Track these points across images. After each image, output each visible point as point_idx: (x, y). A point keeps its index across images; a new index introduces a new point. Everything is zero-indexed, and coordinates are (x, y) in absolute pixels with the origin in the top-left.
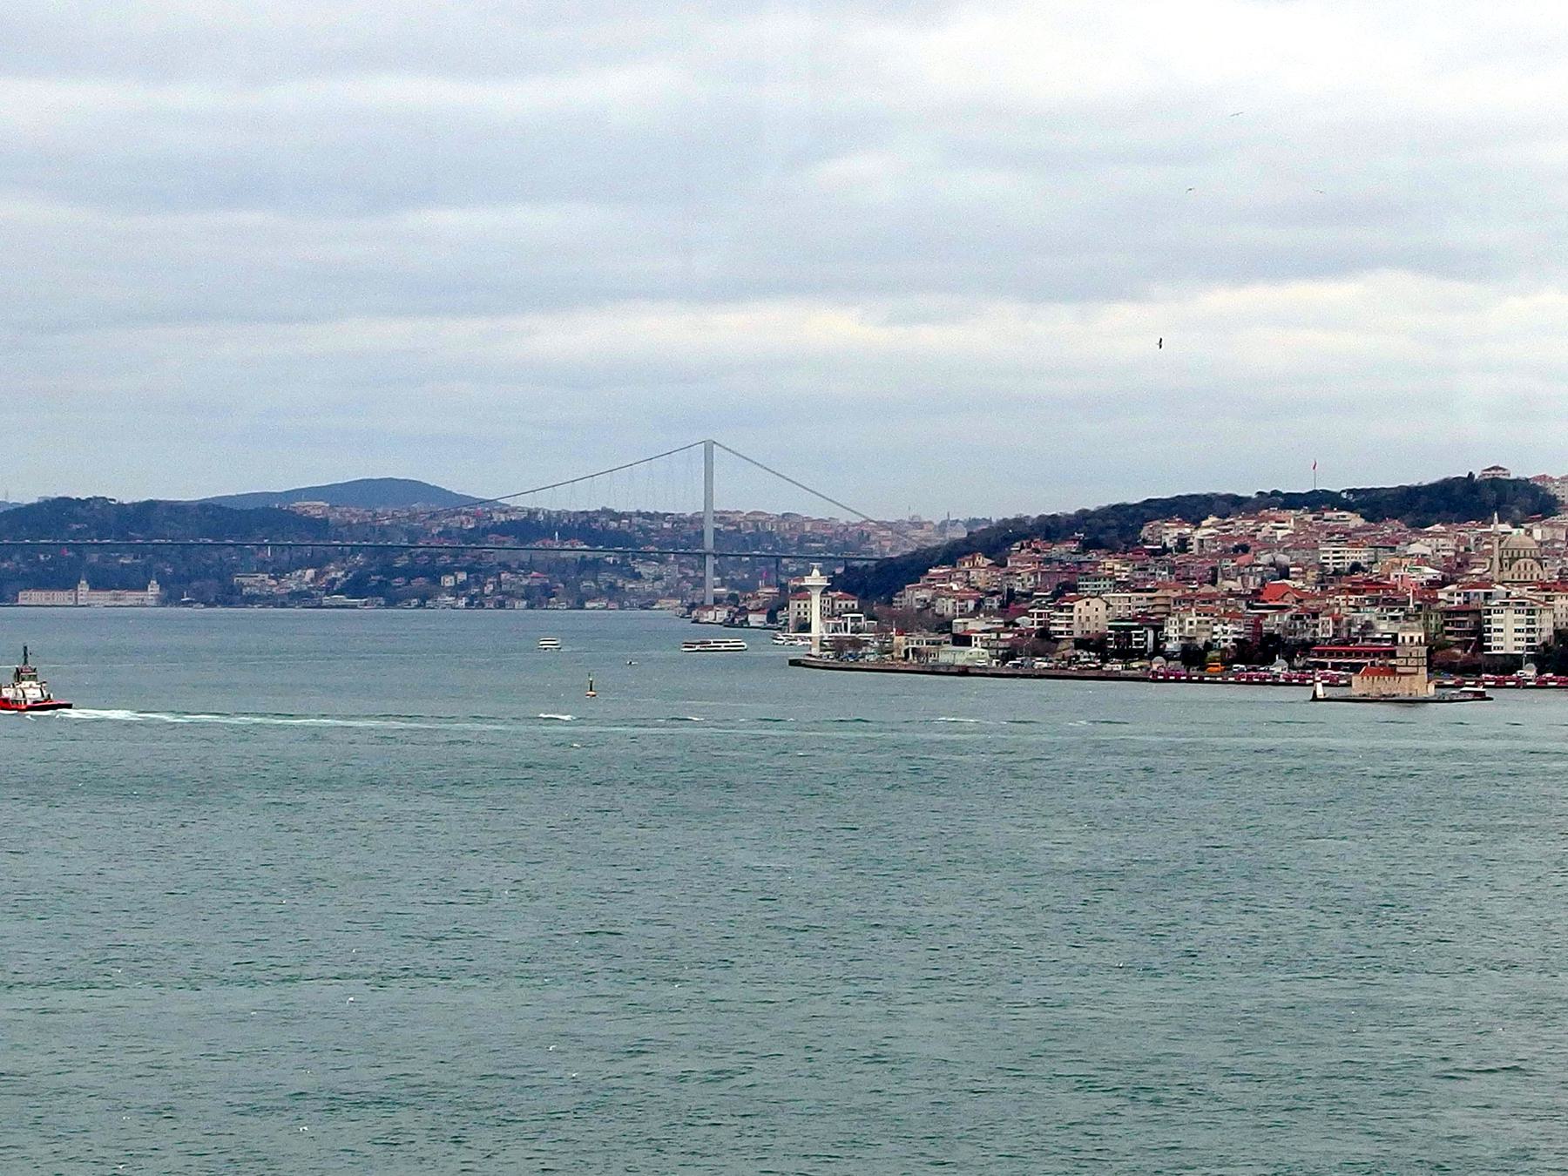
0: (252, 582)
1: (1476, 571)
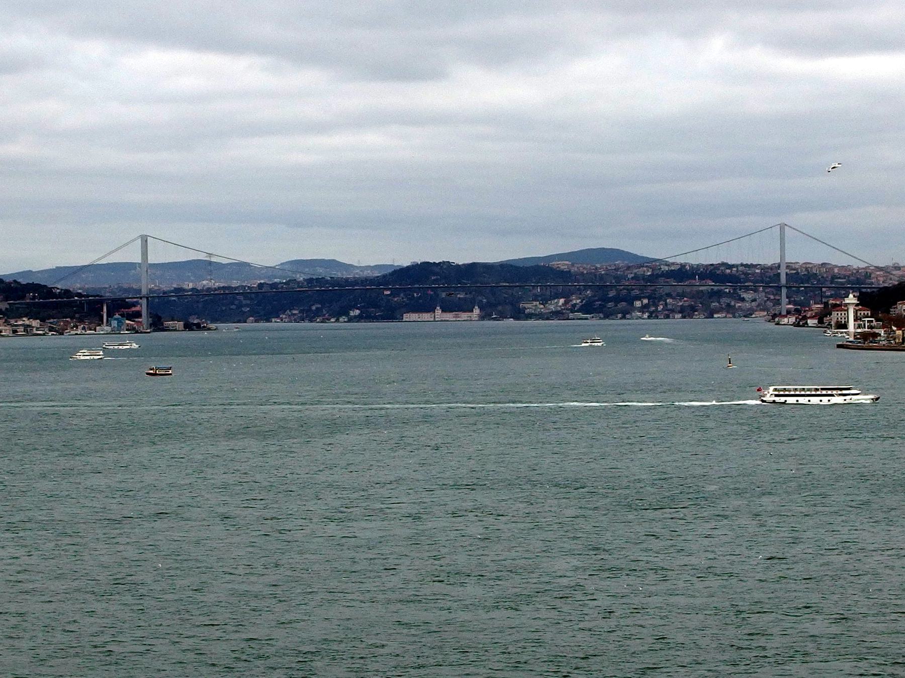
0: (530, 306)
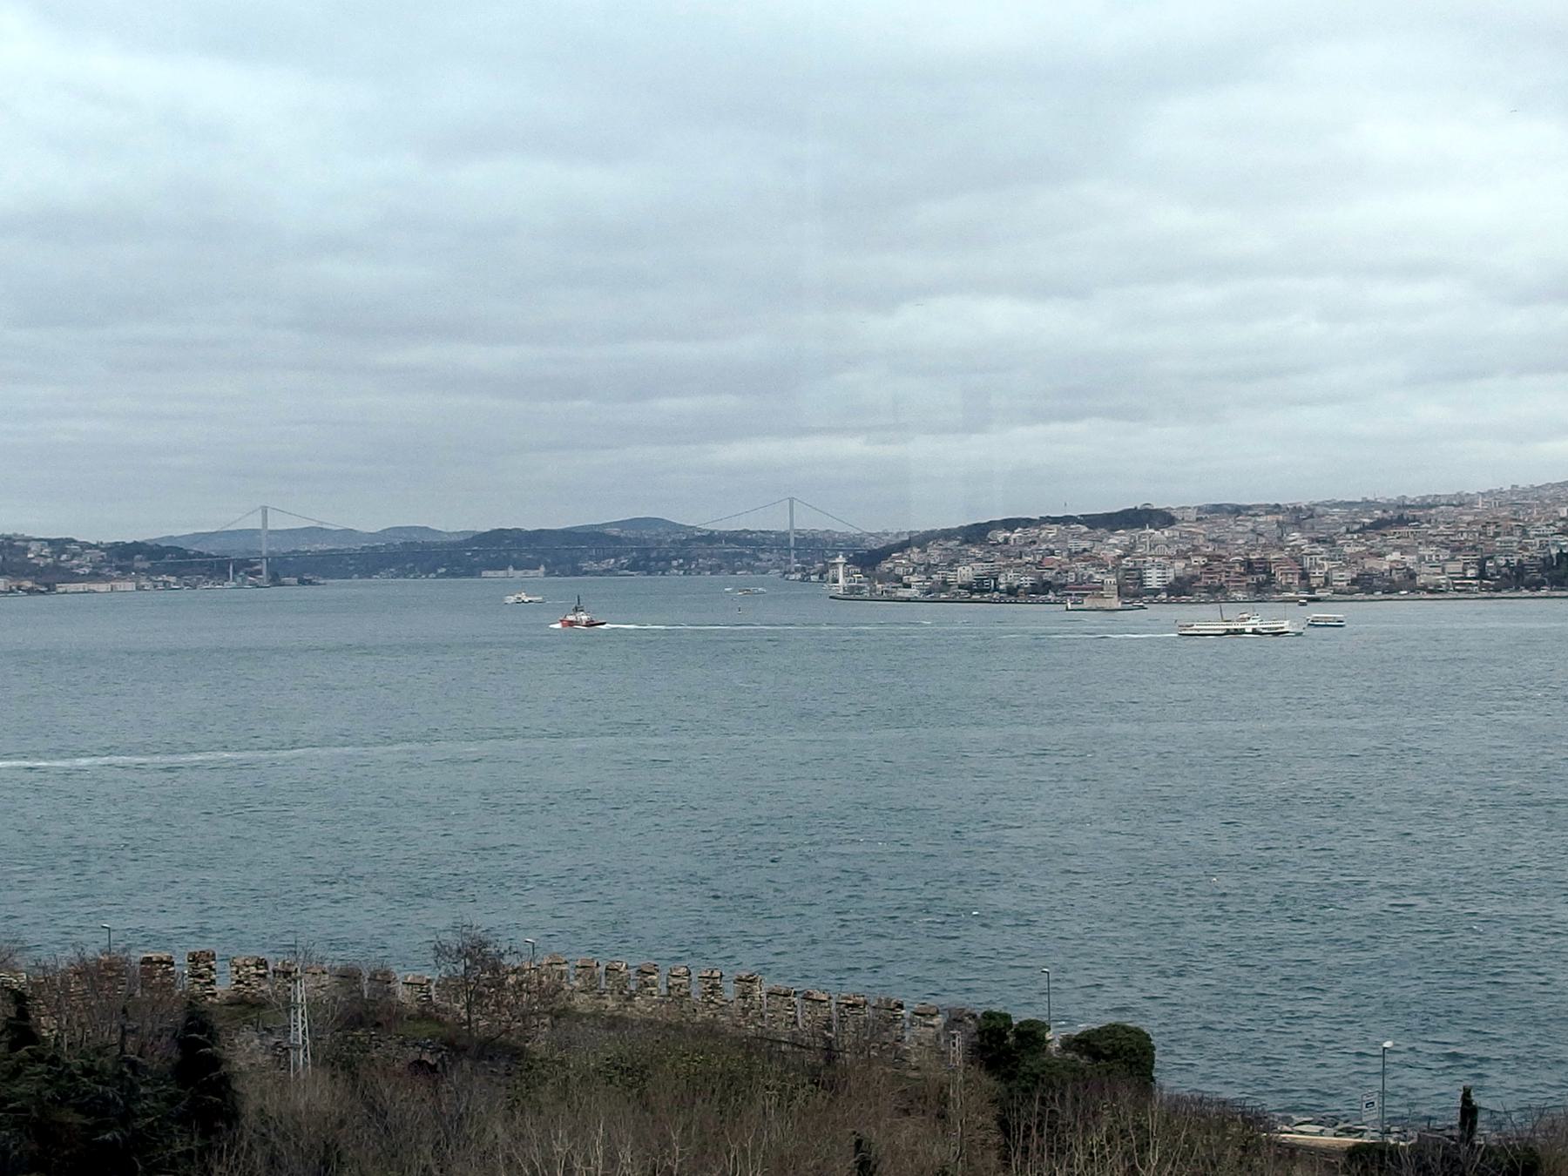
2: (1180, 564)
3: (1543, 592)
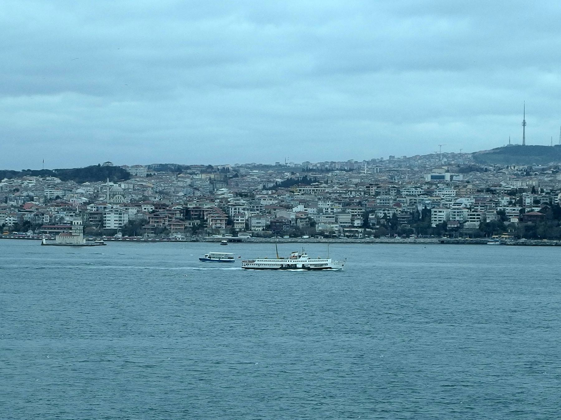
1: (101, 199)
2: (133, 211)
3: (412, 239)
